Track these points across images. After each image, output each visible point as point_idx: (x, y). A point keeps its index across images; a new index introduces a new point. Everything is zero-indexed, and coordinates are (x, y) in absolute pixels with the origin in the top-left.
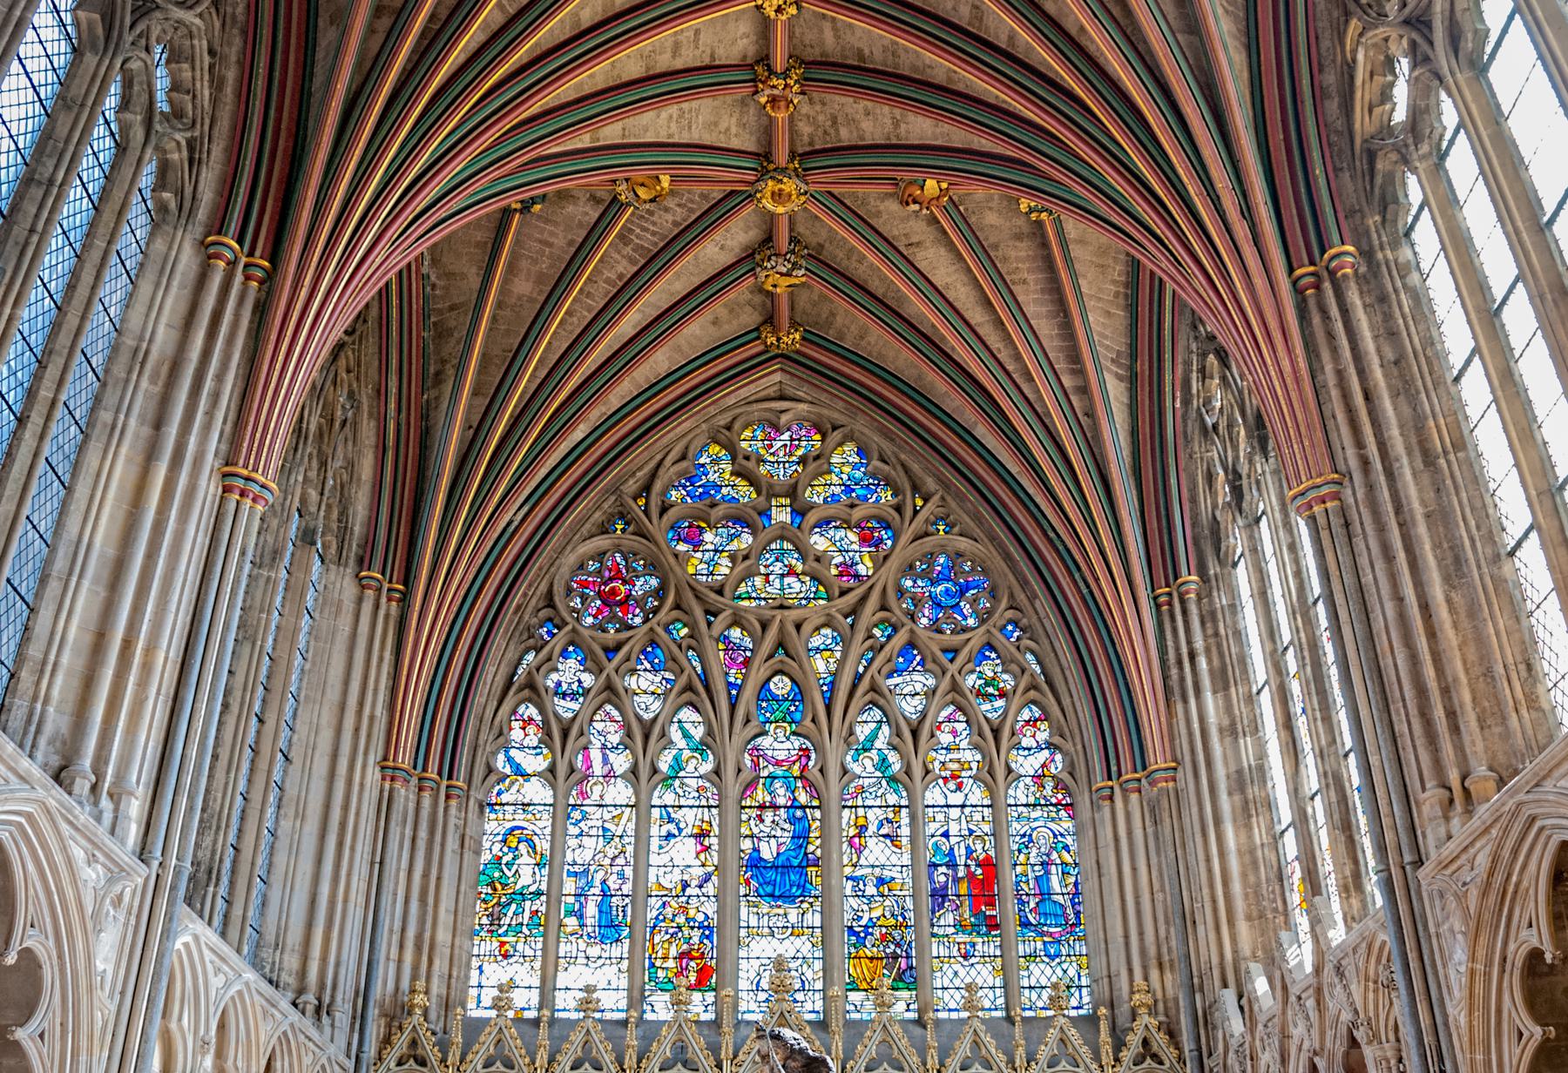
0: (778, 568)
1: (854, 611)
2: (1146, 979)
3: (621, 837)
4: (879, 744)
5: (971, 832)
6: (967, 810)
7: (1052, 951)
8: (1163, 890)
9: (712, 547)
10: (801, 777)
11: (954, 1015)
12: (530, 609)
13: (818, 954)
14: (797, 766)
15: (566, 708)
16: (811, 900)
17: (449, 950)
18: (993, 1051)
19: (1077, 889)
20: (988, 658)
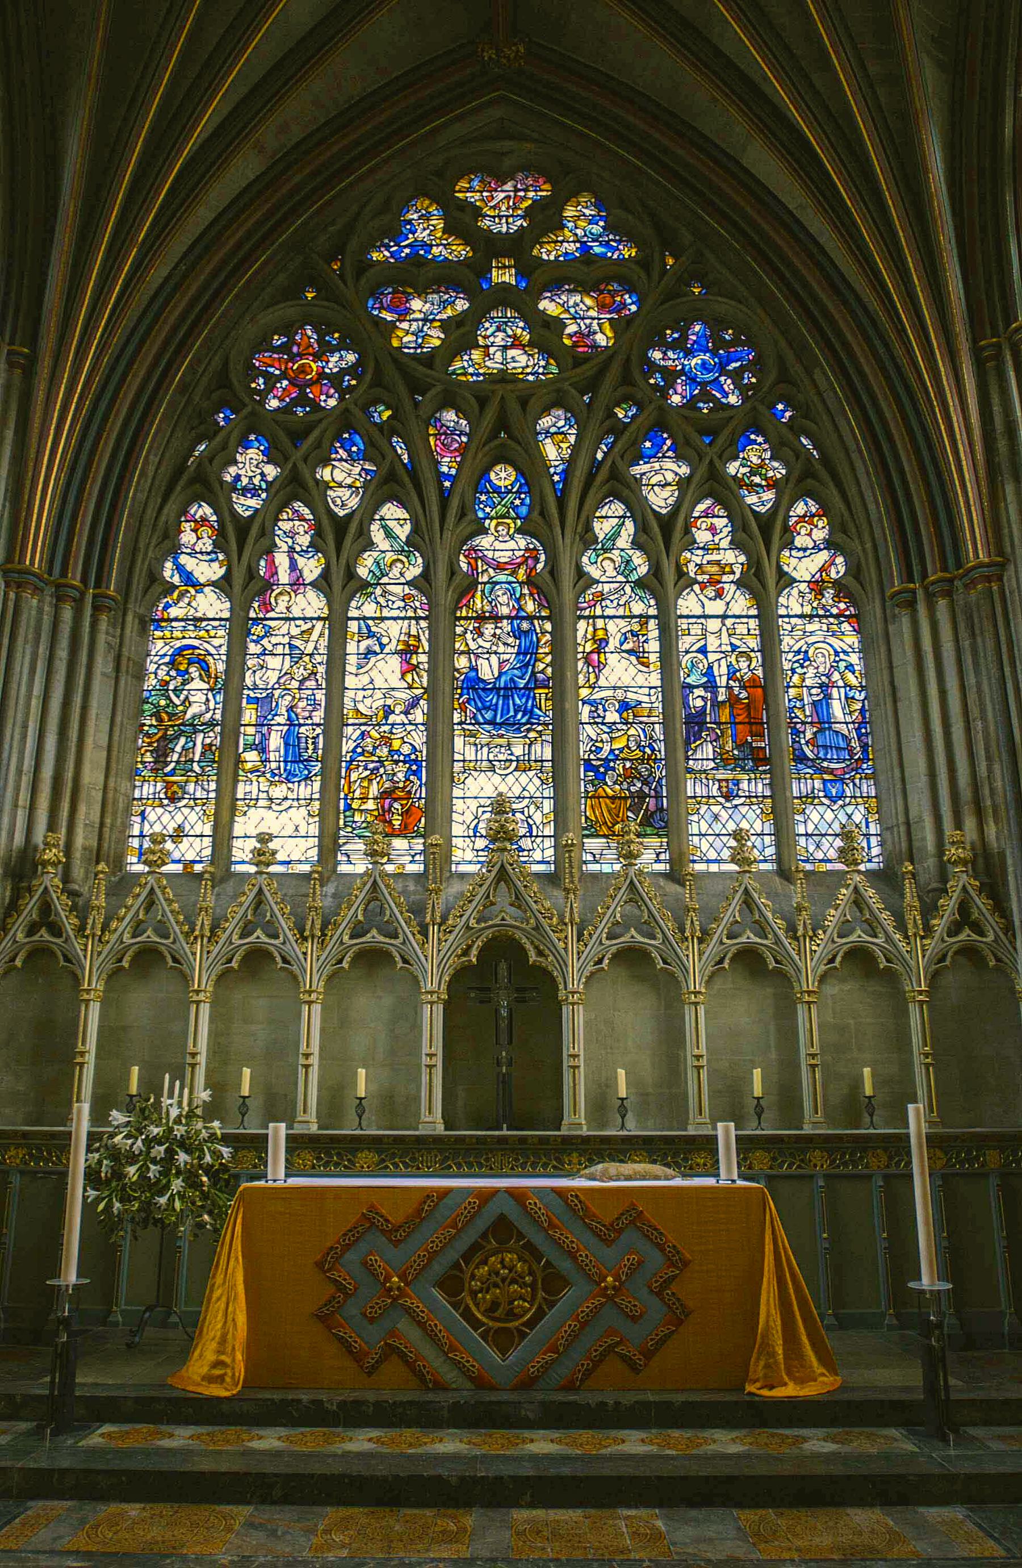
2: (959, 825)
3: (311, 655)
5: (734, 648)
6: (729, 622)
7: (834, 792)
8: (984, 718)
9: (421, 316)
10: (529, 582)
11: (714, 868)
12: (200, 390)
14: (522, 572)
15: (246, 505)
16: (540, 728)
17: (100, 794)
18: (769, 915)
19: (864, 717)
20: (754, 442)
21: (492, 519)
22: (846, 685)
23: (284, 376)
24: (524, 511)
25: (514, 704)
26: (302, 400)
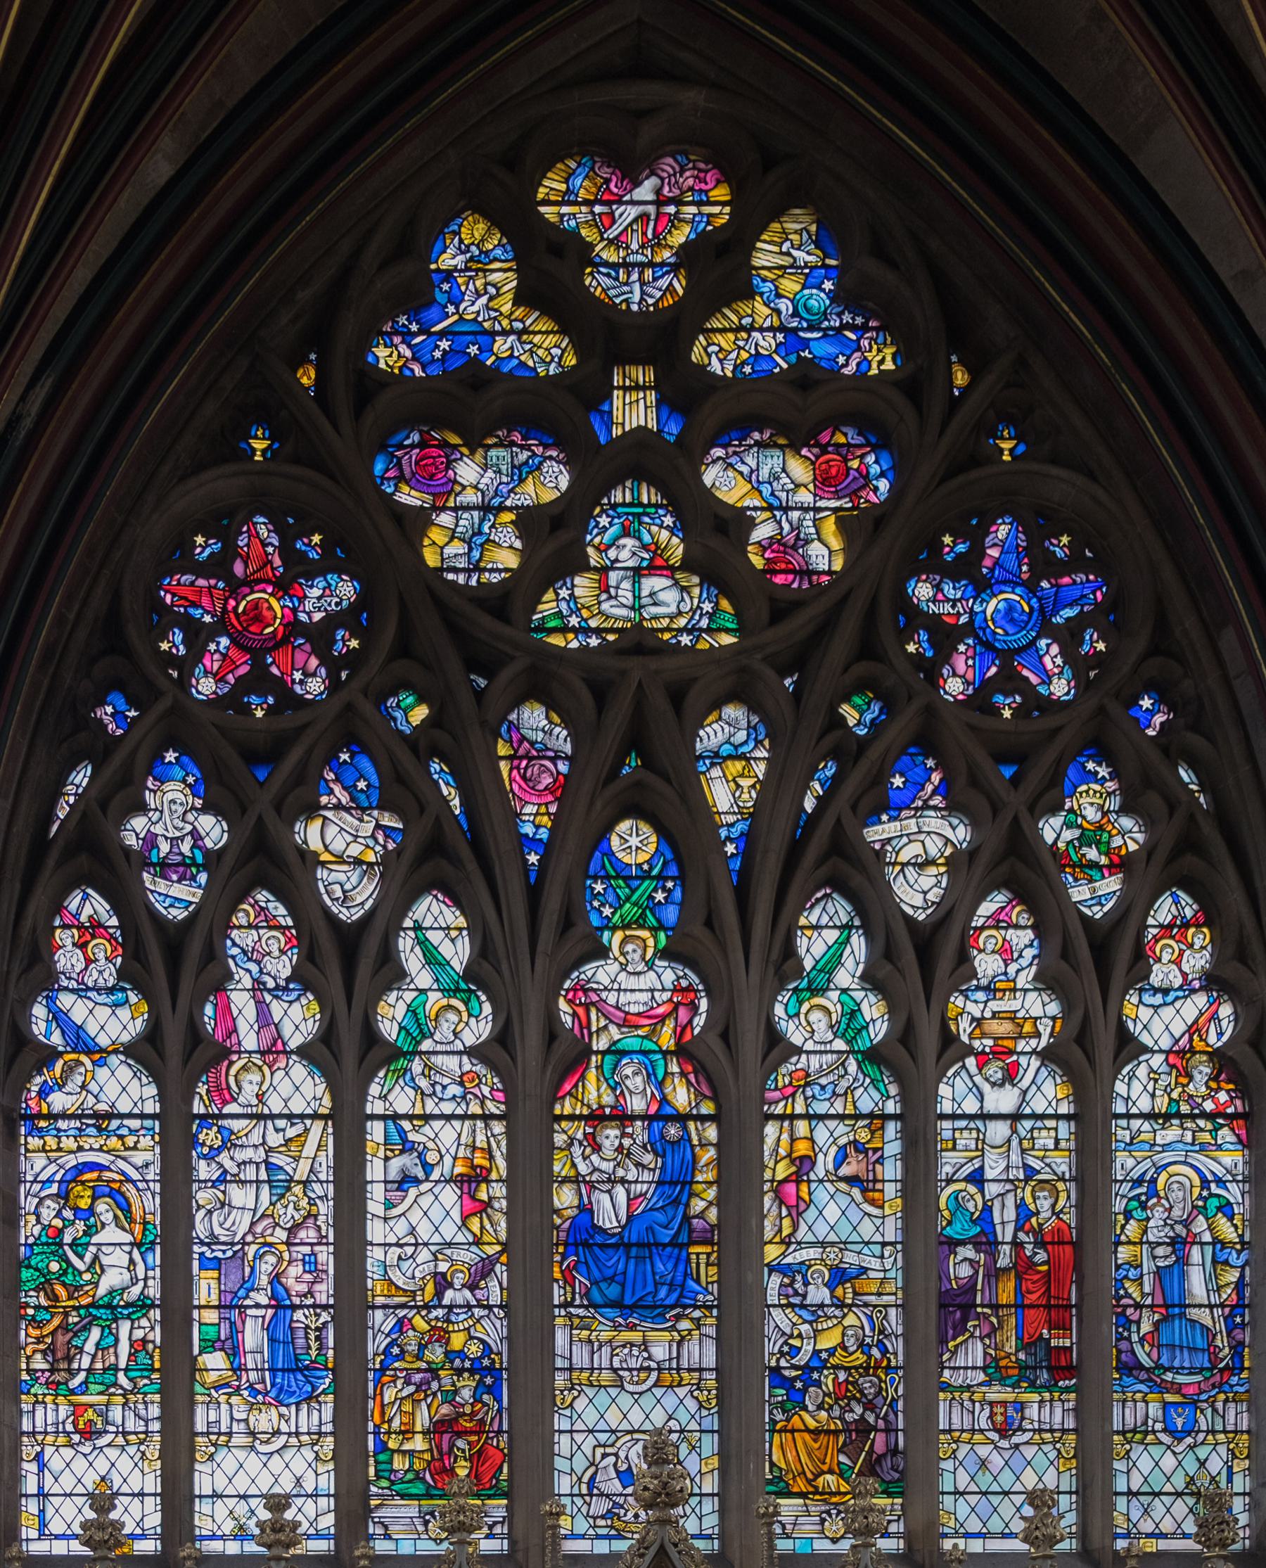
0: (627, 553)
1: (799, 661)
3: (306, 1183)
4: (843, 978)
5: (1030, 1172)
7: (1179, 1422)
10: (682, 1051)
11: (976, 1546)
13: (713, 1422)
14: (667, 1030)
16: (697, 1314)
21: (614, 929)
22: (1216, 1241)
23: (222, 626)
24: (671, 915)
25: (654, 1273)
26: (259, 680)
